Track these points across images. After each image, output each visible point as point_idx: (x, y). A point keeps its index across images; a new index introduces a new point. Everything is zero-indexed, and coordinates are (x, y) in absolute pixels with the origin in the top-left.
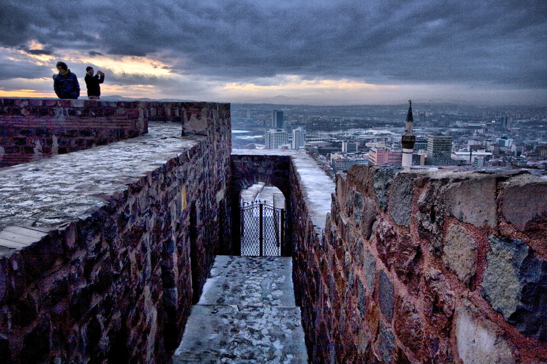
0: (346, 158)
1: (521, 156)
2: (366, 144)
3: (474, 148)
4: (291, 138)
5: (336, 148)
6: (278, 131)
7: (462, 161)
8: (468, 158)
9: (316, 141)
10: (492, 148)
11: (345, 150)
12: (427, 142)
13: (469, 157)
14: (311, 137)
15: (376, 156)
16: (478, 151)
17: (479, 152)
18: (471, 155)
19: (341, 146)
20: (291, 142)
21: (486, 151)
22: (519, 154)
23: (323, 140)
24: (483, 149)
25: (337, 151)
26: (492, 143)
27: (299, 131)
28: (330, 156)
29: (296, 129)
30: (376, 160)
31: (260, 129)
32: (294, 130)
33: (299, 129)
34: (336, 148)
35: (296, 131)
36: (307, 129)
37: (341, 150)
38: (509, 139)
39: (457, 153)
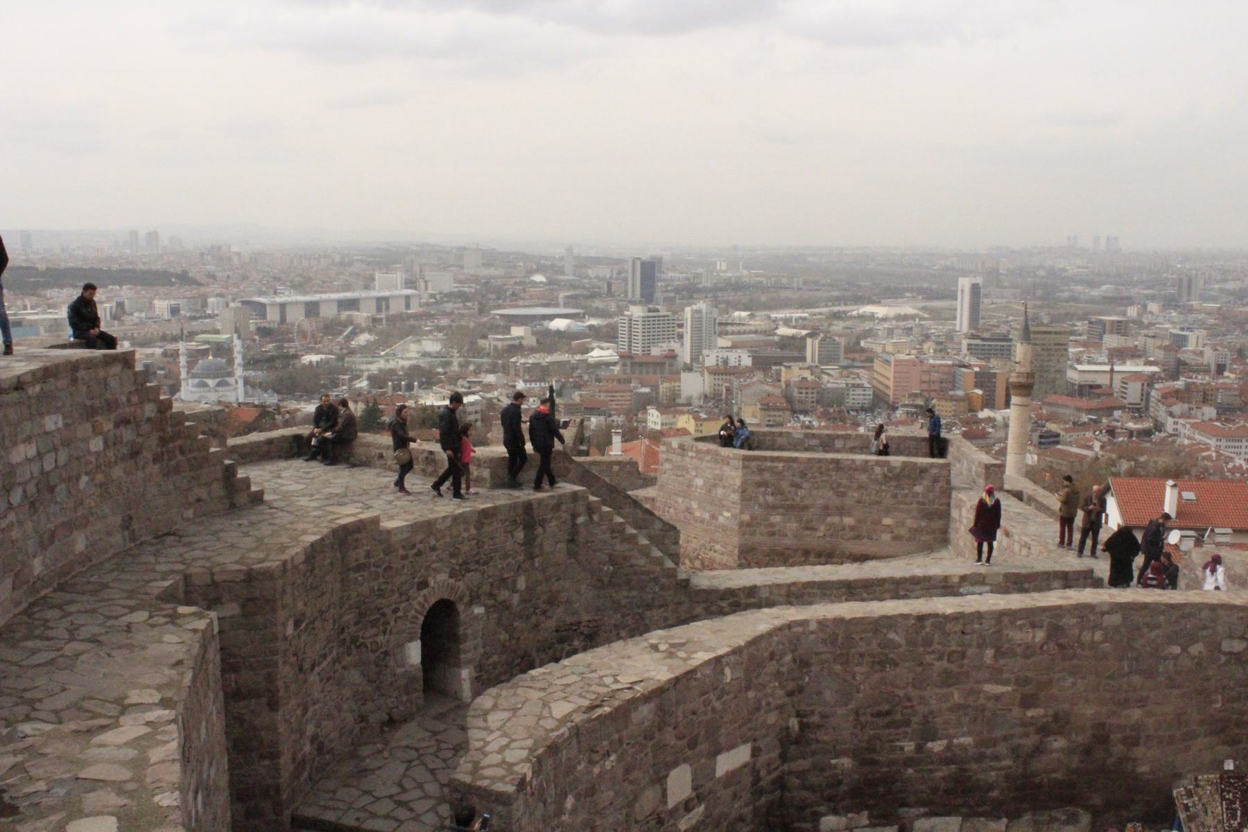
0: (819, 378)
1: (1226, 374)
2: (862, 343)
3: (1120, 354)
4: (681, 326)
5: (787, 353)
6: (650, 311)
7: (1091, 387)
8: (1103, 380)
9: (739, 333)
10: (1159, 355)
11: (813, 361)
12: (1011, 340)
13: (1108, 376)
14: (726, 324)
15: (891, 375)
16: (1128, 362)
17: (1129, 367)
18: (1112, 371)
19: (804, 348)
20: (681, 336)
21: (1146, 363)
22: (1221, 369)
23: (756, 332)
24: (1139, 356)
25: (796, 359)
26: (1158, 342)
27: (699, 311)
28: (779, 373)
29: (695, 307)
30: (891, 384)
31: (598, 304)
32: (688, 310)
33: (702, 305)
34: (787, 353)
35: (694, 312)
36: (716, 303)
37: (803, 359)
38: (1197, 332)
39: (1080, 367)
